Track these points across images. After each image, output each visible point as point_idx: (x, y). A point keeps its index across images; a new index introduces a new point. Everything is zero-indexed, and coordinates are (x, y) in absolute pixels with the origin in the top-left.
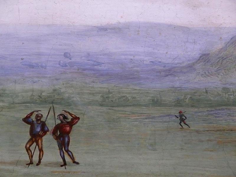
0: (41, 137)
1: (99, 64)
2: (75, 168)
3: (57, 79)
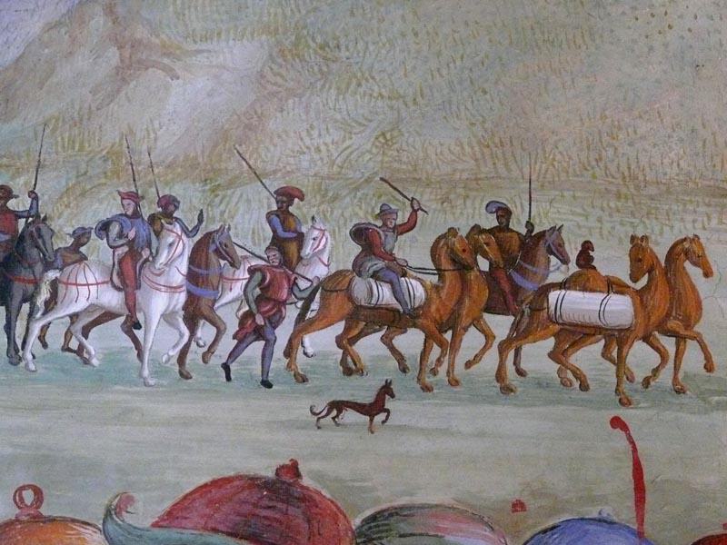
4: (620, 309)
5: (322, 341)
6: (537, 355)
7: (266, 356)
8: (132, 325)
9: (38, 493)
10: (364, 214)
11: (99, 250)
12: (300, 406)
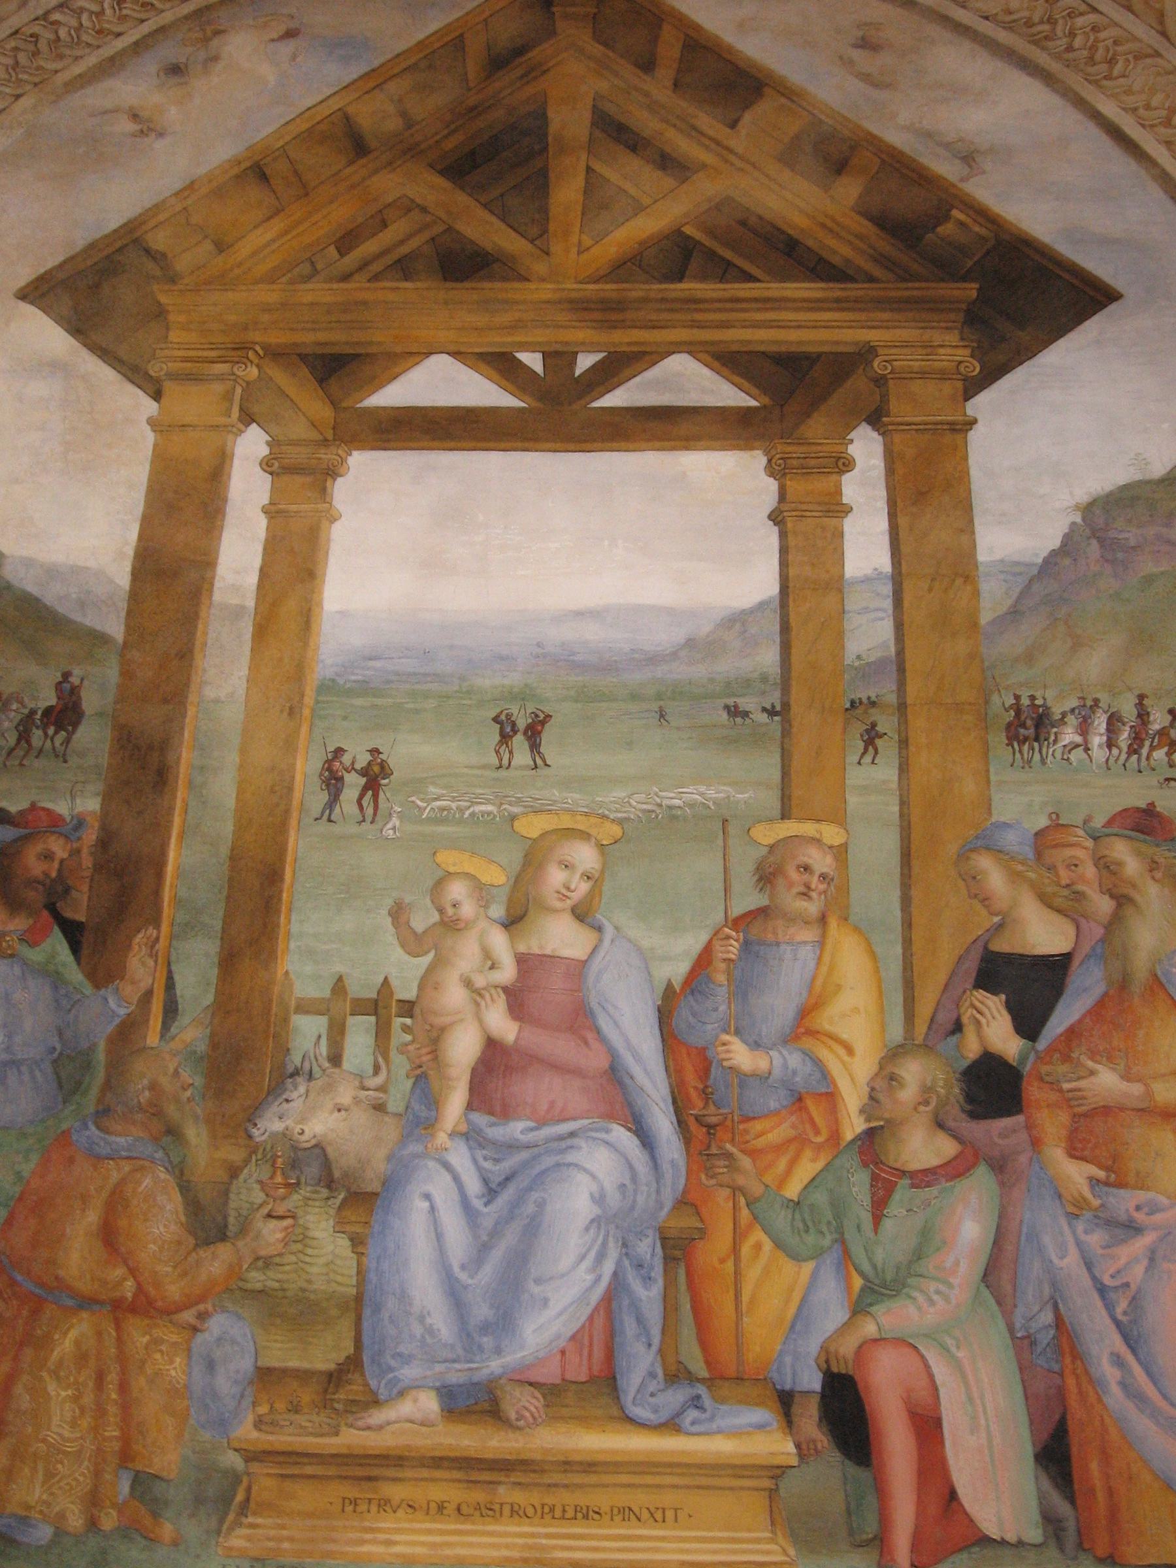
0: (511, 737)
1: (574, 654)
2: (546, 771)
3: (528, 673)
5: (1160, 754)
7: (1139, 760)
8: (1087, 750)
9: (1057, 815)
11: (1072, 720)
12: (1154, 780)
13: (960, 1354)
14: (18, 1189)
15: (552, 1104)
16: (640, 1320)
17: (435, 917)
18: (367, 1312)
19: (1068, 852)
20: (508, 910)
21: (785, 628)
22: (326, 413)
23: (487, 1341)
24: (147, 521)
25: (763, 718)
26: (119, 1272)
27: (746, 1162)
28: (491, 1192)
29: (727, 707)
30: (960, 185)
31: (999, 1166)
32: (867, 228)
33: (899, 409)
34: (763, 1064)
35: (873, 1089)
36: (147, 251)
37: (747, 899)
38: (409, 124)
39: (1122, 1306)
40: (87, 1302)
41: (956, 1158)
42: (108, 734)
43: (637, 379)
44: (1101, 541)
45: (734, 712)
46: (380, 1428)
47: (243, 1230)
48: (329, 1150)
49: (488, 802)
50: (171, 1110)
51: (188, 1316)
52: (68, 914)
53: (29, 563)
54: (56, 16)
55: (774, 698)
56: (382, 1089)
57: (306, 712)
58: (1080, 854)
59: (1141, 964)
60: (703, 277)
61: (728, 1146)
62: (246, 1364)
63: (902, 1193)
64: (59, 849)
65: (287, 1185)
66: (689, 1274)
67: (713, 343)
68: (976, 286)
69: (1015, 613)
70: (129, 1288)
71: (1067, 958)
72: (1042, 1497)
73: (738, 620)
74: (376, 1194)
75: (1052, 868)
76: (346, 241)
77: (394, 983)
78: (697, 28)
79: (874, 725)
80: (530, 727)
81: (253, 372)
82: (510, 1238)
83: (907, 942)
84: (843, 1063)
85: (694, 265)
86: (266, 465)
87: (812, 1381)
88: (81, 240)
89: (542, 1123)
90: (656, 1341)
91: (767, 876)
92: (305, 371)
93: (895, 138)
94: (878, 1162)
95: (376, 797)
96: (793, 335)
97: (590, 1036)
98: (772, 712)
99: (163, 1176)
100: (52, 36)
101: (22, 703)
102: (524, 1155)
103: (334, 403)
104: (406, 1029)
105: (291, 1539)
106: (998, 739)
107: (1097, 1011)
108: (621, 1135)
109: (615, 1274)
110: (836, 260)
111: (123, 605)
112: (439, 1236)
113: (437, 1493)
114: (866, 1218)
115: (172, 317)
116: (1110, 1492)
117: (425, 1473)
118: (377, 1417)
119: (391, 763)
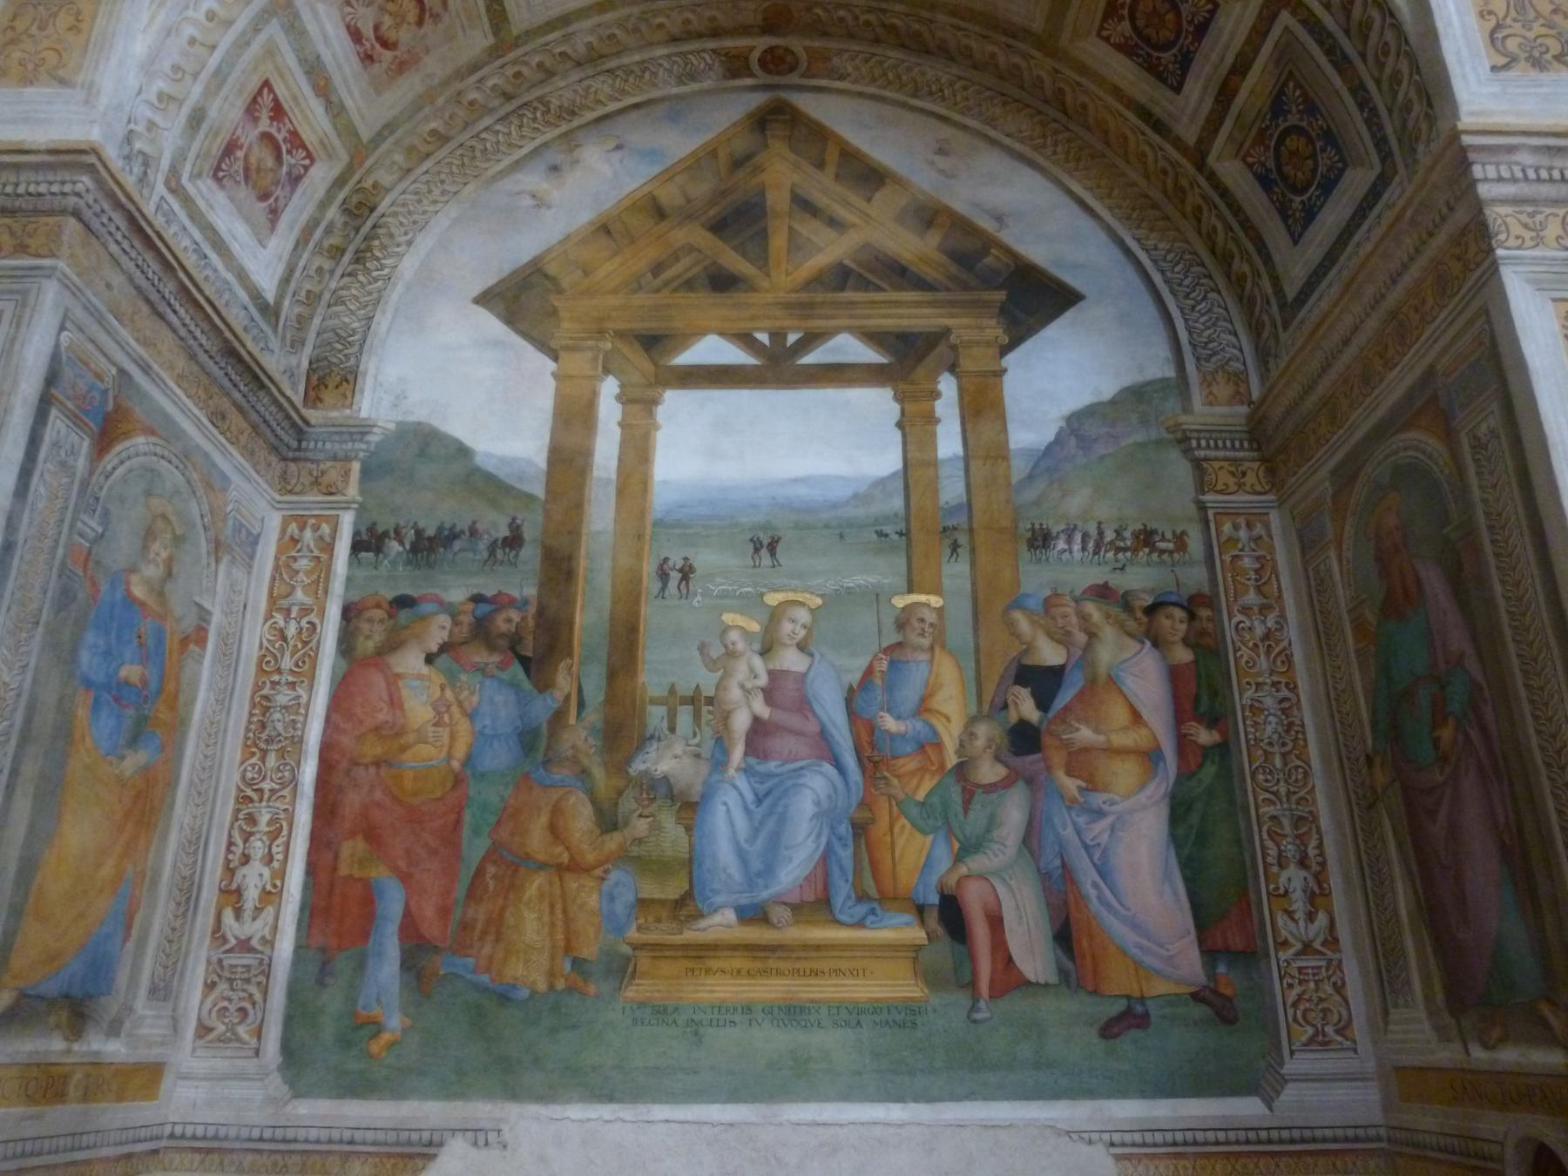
4: (1171, 546)
5: (1110, 555)
6: (1155, 556)
10: (1116, 526)
11: (1063, 537)
12: (1107, 569)
13: (1013, 883)
14: (502, 806)
15: (790, 752)
16: (841, 868)
17: (723, 651)
18: (695, 867)
19: (1064, 609)
20: (763, 644)
21: (907, 487)
22: (652, 368)
23: (760, 881)
24: (554, 431)
25: (896, 537)
26: (560, 849)
27: (895, 781)
28: (759, 801)
29: (877, 532)
30: (996, 234)
31: (1030, 781)
32: (943, 259)
33: (966, 364)
34: (903, 728)
35: (961, 741)
36: (546, 276)
37: (892, 638)
38: (689, 201)
39: (1097, 856)
40: (542, 866)
41: (1007, 777)
42: (539, 551)
43: (821, 348)
44: (1077, 436)
45: (881, 534)
46: (705, 930)
47: (626, 824)
48: (672, 780)
49: (749, 586)
50: (586, 762)
51: (598, 872)
52: (523, 653)
53: (490, 456)
54: (484, 135)
55: (902, 526)
56: (698, 745)
57: (647, 538)
58: (1069, 610)
59: (1102, 670)
60: (856, 289)
61: (886, 773)
62: (631, 897)
63: (979, 796)
64: (515, 616)
65: (649, 799)
66: (867, 844)
67: (861, 327)
68: (1004, 292)
69: (1031, 477)
70: (565, 858)
71: (1062, 668)
72: (1058, 962)
73: (881, 483)
74: (697, 803)
75: (1054, 618)
76: (657, 269)
77: (702, 687)
78: (847, 143)
79: (956, 541)
80: (769, 544)
81: (609, 345)
82: (771, 825)
83: (978, 662)
84: (947, 729)
85: (851, 281)
86: (619, 398)
87: (934, 899)
88: (507, 269)
89: (785, 762)
90: (851, 879)
91: (901, 624)
92: (637, 345)
93: (959, 206)
94: (966, 780)
95: (687, 584)
96: (905, 322)
97: (809, 715)
98: (901, 534)
99: (582, 795)
100: (482, 147)
101: (489, 533)
102: (776, 780)
103: (655, 364)
104: (710, 712)
105: (658, 991)
106: (1023, 548)
107: (1081, 693)
108: (828, 768)
109: (828, 843)
110: (929, 279)
111: (543, 478)
112: (732, 824)
113: (737, 963)
114: (960, 809)
115: (563, 314)
116: (1093, 957)
117: (729, 953)
118: (704, 923)
119: (695, 565)
